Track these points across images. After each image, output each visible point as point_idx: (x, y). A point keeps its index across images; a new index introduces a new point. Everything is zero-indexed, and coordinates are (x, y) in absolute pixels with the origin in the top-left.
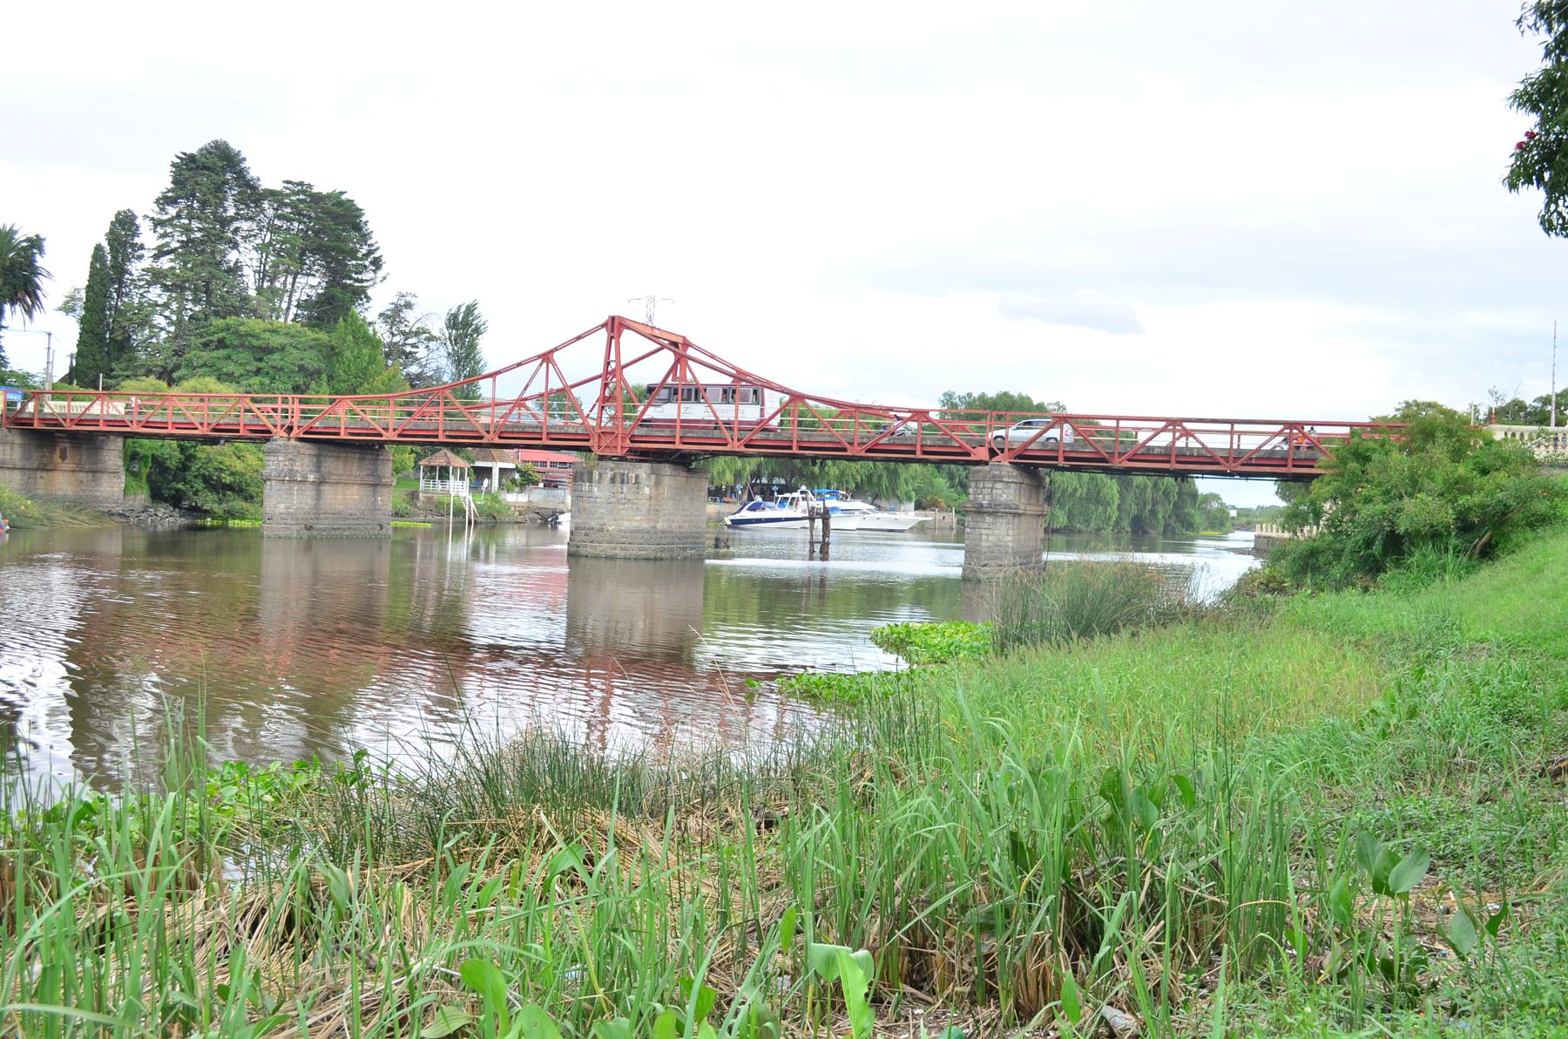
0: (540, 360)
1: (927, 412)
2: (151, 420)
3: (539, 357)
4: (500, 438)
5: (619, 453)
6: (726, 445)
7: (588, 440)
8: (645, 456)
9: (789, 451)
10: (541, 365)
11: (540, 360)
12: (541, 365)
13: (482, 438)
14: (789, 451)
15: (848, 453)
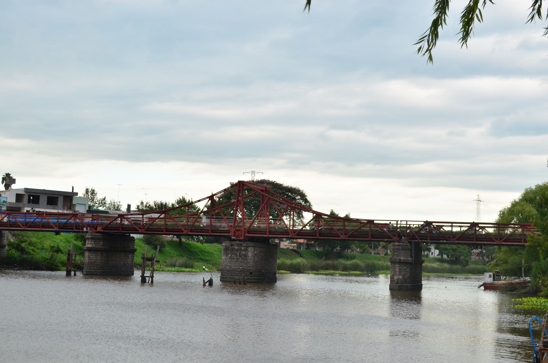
0: (208, 199)
1: (373, 221)
2: (32, 224)
3: (208, 198)
4: (191, 232)
5: (242, 238)
6: (289, 235)
7: (229, 233)
8: (252, 239)
9: (316, 237)
10: (209, 201)
11: (208, 199)
12: (209, 201)
13: (183, 232)
14: (316, 237)
15: (340, 238)
